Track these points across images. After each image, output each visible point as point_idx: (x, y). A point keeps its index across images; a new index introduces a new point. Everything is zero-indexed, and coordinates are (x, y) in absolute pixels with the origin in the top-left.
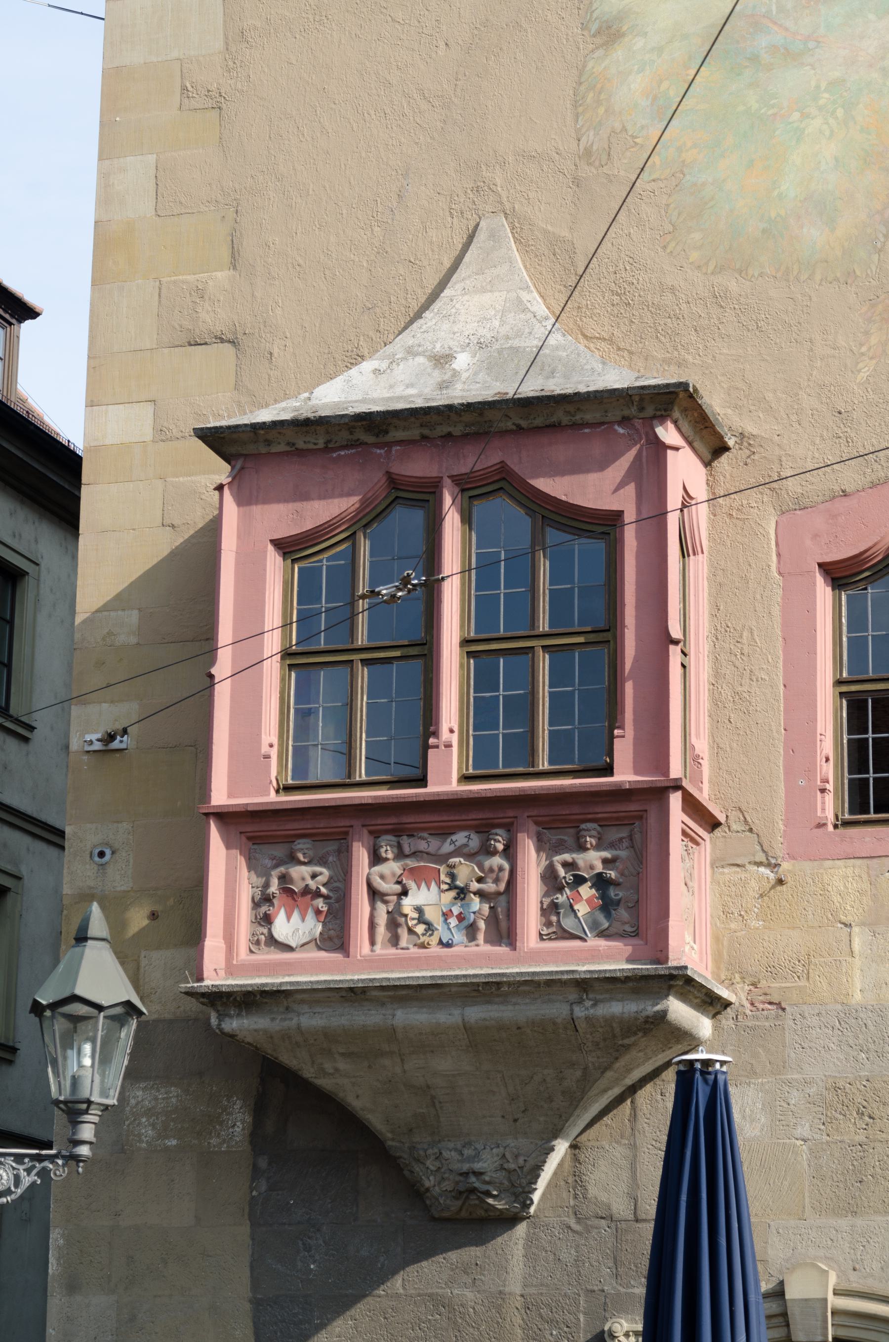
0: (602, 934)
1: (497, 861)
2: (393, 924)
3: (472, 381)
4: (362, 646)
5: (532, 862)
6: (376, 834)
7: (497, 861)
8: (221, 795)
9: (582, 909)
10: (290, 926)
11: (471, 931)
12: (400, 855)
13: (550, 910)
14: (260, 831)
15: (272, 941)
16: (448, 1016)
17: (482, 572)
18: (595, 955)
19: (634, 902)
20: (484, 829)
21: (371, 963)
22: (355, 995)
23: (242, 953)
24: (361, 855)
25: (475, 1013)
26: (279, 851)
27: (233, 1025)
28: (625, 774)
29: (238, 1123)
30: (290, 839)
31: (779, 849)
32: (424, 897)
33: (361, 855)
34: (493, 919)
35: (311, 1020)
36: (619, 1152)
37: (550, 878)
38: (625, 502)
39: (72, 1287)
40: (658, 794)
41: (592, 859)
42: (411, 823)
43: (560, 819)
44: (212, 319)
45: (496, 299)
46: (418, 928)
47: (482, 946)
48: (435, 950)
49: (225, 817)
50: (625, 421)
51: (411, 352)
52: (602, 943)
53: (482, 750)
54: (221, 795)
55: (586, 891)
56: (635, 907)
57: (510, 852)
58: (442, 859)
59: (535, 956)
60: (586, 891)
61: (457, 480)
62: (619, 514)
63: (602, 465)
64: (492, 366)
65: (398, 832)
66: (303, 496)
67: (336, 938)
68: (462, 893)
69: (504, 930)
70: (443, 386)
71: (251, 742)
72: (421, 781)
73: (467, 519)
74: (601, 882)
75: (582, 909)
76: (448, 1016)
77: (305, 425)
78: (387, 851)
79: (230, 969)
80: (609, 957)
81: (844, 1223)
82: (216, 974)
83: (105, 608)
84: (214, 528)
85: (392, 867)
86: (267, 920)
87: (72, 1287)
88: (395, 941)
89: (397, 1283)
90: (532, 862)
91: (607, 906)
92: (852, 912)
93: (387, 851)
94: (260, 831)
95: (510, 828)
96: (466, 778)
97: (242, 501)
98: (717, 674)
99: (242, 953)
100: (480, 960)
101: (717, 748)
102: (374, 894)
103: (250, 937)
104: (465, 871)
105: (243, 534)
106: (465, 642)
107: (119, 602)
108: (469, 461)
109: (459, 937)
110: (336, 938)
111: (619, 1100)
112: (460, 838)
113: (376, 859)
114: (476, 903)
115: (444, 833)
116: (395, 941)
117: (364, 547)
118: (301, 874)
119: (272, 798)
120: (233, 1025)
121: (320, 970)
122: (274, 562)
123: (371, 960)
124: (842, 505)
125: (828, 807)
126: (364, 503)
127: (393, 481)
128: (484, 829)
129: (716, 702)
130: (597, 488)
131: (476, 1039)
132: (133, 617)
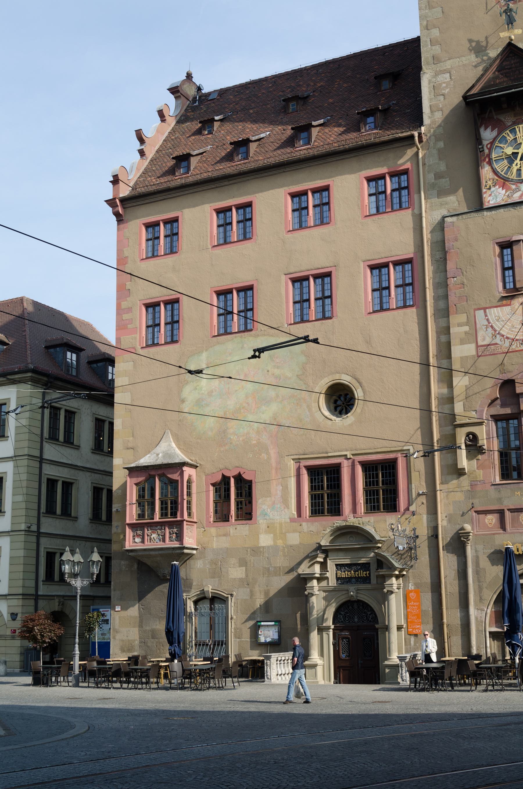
0: (176, 541)
1: (163, 530)
2: (150, 540)
3: (160, 461)
4: (145, 499)
5: (167, 531)
6: (148, 527)
7: (163, 530)
8: (128, 521)
9: (174, 537)
10: (138, 540)
11: (160, 540)
12: (151, 530)
13: (170, 537)
14: (133, 526)
15: (135, 542)
16: (157, 553)
17: (162, 489)
18: (175, 544)
19: (180, 537)
20: (161, 526)
21: (148, 545)
22: (145, 550)
23: (131, 544)
24: (146, 530)
25: (160, 552)
26: (136, 529)
27: (130, 554)
28: (179, 519)
29: (136, 566)
30: (137, 527)
31: (205, 525)
32: (154, 536)
33: (146, 530)
34: (163, 539)
35: (140, 553)
36: (184, 570)
37: (170, 533)
38: (179, 478)
39: (114, 590)
40: (182, 521)
41: (175, 530)
42: (153, 526)
43: (171, 525)
44: (130, 445)
45: (167, 444)
46: (153, 541)
47: (161, 543)
48: (155, 543)
49: (128, 524)
50: (179, 466)
51: (154, 453)
52: (176, 542)
53: (162, 515)
54: (128, 521)
55: (174, 535)
56: (180, 537)
57: (165, 529)
58: (156, 530)
59: (168, 544)
60: (174, 535)
61: (159, 475)
62: (178, 480)
63: (176, 473)
64: (164, 457)
65: (151, 526)
66: (138, 477)
67: (143, 542)
68: (159, 535)
69: (164, 541)
70: (157, 460)
71: (132, 514)
72: (153, 519)
73: (160, 480)
74: (176, 533)
75: (174, 537)
76: (157, 553)
77: (137, 467)
78: (149, 529)
79: (130, 546)
80: (176, 545)
81: (213, 579)
82: (127, 547)
83: (117, 490)
84: (126, 482)
85: (150, 531)
86: (134, 539)
87: (114, 590)
88: (150, 542)
89: (156, 589)
90: (167, 531)
91: (177, 537)
92: (214, 535)
93: (149, 529)
94: (133, 526)
95: (165, 526)
96: (159, 518)
97: (130, 477)
98: (197, 500)
99: (131, 544)
100: (160, 545)
101: (197, 511)
102: (148, 535)
103: (131, 542)
104: (159, 531)
105: (130, 482)
106: (159, 498)
107: (118, 489)
108: (160, 472)
109: (158, 541)
110: (143, 542)
111: (184, 562)
112: (159, 527)
113: (148, 530)
114: (160, 536)
115: (156, 526)
116: (150, 542)
117: (146, 484)
118: (138, 532)
119: (135, 521)
120: (130, 554)
121: (141, 547)
122: (135, 487)
123: (148, 545)
124: (213, 475)
125: (212, 519)
126: (146, 478)
127: (150, 475)
128: (161, 526)
129: (197, 504)
130: (175, 476)
131: (161, 555)
132: (120, 491)
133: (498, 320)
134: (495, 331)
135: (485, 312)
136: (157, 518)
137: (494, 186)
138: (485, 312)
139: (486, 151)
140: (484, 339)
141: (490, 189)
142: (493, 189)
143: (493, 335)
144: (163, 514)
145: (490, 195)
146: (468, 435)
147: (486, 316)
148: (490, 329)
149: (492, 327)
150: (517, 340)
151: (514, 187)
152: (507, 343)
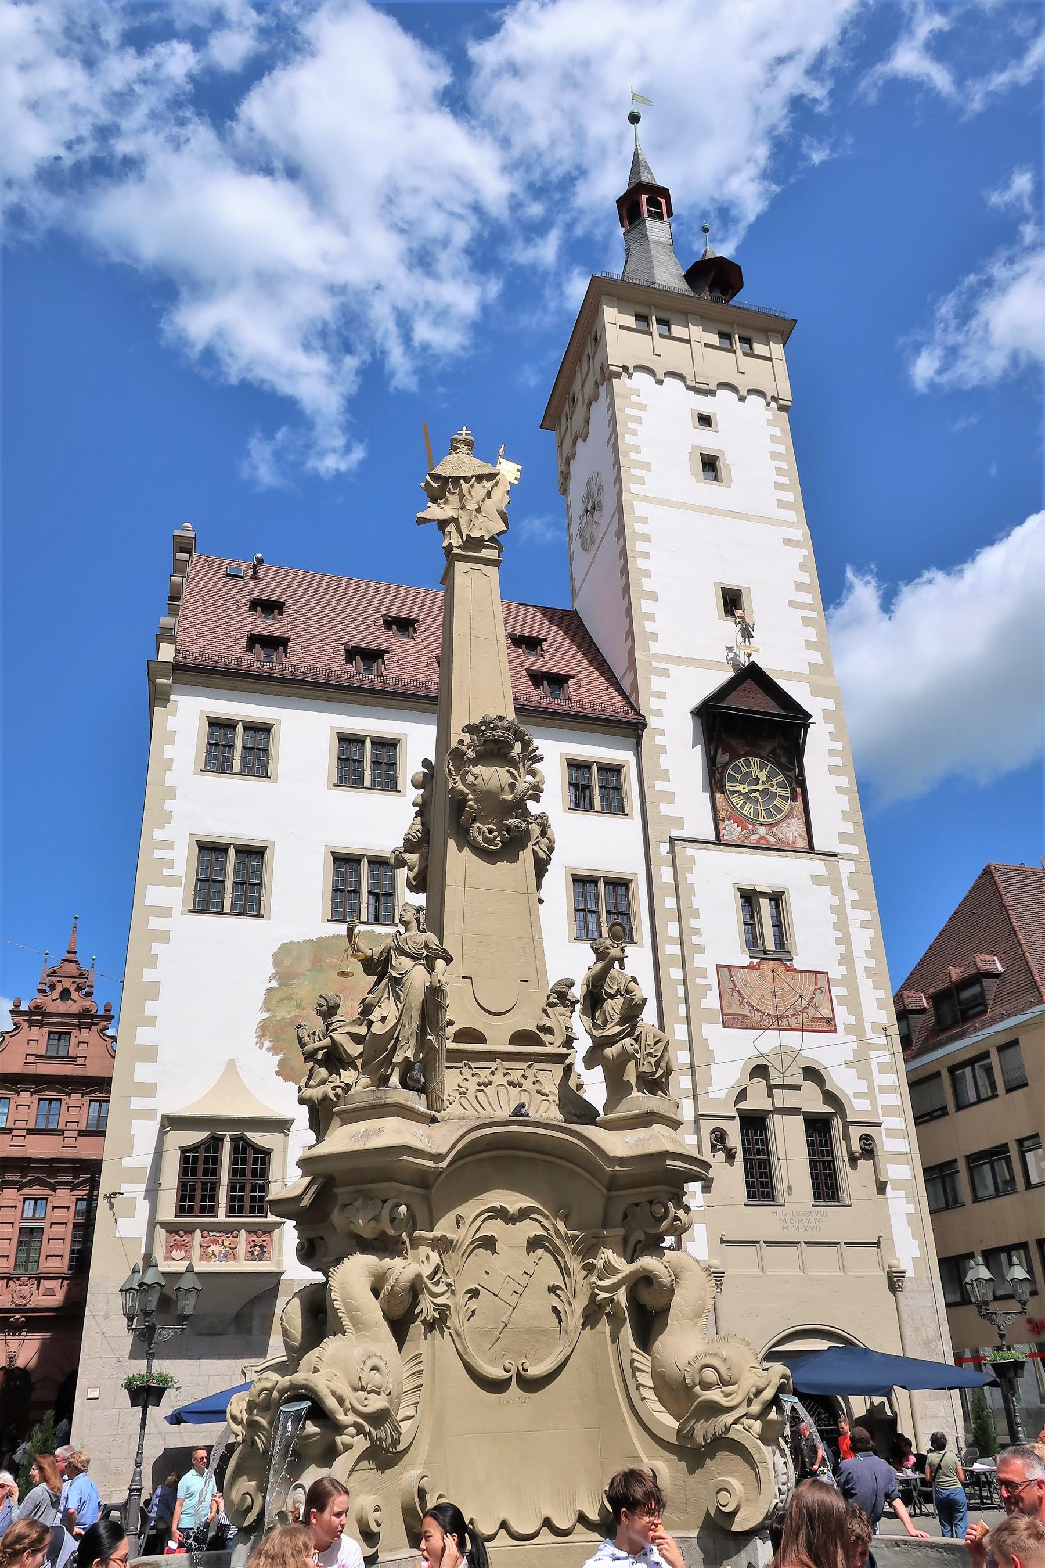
55: (257, 1248)
133: (745, 985)
134: (743, 998)
135: (730, 972)
136: (222, 1216)
137: (728, 819)
138: (730, 972)
139: (718, 775)
140: (730, 1006)
141: (723, 821)
142: (727, 822)
143: (741, 1003)
144: (231, 1210)
145: (724, 829)
146: (713, 1132)
147: (731, 977)
148: (736, 995)
149: (738, 991)
150: (768, 1015)
151: (750, 827)
152: (757, 1017)
